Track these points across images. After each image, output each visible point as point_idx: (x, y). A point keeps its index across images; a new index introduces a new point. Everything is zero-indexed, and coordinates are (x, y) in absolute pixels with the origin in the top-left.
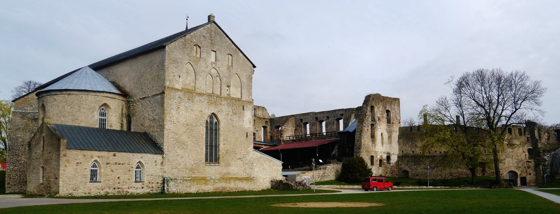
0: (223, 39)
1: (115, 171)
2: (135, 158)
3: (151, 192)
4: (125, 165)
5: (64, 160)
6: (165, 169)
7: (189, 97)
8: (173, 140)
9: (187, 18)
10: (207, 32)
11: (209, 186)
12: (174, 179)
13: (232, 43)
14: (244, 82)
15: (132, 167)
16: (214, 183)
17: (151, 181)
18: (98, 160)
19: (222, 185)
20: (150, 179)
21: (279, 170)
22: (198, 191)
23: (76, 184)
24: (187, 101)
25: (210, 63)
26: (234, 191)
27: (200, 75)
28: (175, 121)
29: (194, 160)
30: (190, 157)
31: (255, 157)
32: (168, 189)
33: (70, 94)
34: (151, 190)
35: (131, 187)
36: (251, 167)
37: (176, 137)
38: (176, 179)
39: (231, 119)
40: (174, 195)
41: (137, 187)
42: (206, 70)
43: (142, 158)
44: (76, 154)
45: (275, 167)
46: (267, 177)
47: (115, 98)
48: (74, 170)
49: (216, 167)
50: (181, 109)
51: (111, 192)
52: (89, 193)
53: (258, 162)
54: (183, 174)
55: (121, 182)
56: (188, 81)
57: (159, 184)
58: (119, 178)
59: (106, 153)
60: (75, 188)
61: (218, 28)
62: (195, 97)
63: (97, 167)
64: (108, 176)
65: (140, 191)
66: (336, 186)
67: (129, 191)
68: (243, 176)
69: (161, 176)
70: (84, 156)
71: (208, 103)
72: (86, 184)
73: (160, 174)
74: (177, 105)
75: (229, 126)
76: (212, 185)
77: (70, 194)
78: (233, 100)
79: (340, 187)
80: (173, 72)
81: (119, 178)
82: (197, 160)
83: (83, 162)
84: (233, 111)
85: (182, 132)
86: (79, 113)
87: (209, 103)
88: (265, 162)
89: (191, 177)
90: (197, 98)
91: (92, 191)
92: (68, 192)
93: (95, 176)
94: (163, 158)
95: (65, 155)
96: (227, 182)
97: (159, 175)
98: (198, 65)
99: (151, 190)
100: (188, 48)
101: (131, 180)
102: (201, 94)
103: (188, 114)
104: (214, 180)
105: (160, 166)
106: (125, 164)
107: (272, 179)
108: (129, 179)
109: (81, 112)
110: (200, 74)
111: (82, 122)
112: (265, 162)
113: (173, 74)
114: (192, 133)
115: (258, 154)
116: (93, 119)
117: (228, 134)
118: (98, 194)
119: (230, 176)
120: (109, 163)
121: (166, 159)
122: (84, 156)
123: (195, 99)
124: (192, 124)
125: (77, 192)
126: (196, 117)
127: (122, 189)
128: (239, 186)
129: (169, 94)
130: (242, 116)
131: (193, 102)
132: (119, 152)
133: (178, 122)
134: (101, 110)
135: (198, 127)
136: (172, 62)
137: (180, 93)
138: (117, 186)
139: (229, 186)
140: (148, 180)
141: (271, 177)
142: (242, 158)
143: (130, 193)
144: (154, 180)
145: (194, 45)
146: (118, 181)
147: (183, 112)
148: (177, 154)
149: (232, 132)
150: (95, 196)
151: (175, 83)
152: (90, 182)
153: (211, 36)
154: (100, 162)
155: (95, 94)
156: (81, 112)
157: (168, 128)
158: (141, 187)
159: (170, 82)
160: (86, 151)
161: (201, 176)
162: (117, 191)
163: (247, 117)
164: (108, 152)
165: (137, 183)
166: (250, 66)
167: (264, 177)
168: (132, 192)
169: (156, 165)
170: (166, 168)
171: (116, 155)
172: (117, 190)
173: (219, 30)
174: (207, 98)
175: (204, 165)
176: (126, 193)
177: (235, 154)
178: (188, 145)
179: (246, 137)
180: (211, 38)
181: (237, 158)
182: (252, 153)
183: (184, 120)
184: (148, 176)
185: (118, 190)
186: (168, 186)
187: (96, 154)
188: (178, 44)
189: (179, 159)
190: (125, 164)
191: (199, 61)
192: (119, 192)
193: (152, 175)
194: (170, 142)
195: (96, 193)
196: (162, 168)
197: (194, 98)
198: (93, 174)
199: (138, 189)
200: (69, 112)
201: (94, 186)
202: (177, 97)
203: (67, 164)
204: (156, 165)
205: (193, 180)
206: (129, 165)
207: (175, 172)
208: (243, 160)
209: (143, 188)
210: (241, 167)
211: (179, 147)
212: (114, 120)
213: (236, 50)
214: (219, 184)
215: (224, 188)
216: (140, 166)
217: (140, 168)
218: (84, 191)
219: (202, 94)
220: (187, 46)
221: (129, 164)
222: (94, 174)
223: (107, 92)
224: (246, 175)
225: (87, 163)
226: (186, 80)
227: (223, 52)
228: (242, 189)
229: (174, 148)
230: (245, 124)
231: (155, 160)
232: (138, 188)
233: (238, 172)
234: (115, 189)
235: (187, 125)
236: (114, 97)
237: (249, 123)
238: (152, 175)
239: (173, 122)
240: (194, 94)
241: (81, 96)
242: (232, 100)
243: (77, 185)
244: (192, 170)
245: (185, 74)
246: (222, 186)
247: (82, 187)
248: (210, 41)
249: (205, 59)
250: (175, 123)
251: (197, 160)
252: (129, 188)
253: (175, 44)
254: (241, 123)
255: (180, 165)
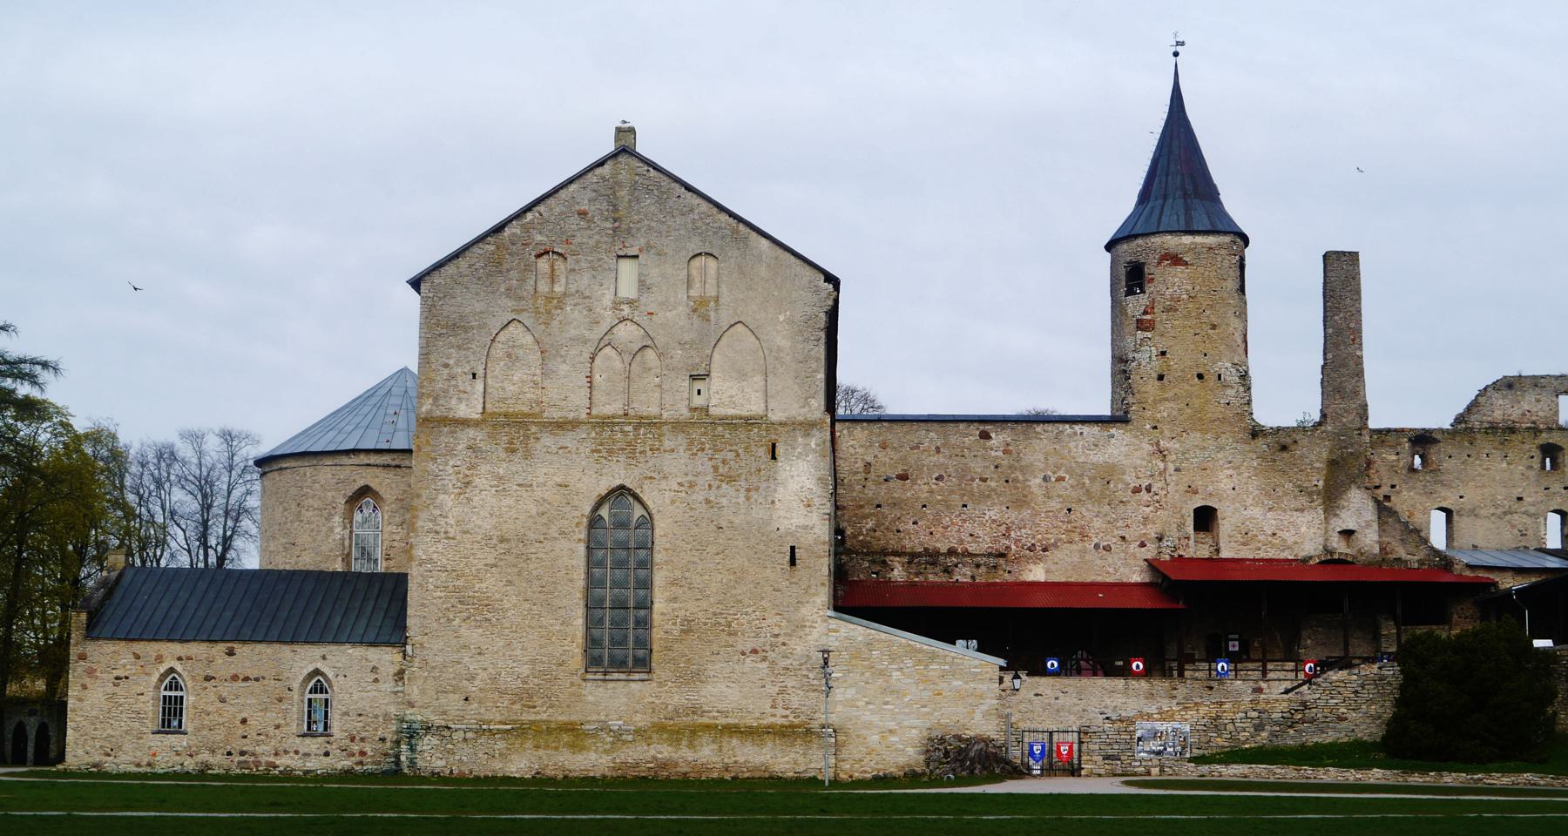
0: (671, 203)
1: (232, 702)
2: (302, 660)
3: (358, 768)
4: (265, 682)
5: (79, 669)
6: (408, 695)
7: (512, 443)
8: (442, 594)
9: (1173, 49)
10: (594, 194)
11: (593, 756)
12: (438, 727)
13: (715, 210)
14: (780, 349)
15: (289, 689)
16: (613, 743)
17: (358, 731)
18: (179, 668)
19: (653, 752)
20: (355, 725)
21: (981, 697)
22: (538, 773)
23: (112, 736)
24: (503, 455)
25: (610, 304)
26: (715, 775)
27: (561, 356)
28: (450, 530)
29: (533, 662)
30: (514, 653)
31: (837, 644)
32: (412, 762)
33: (281, 469)
34: (357, 764)
35: (286, 752)
36: (815, 682)
37: (457, 583)
38: (449, 728)
39: (708, 501)
40: (436, 777)
41: (306, 750)
42: (587, 333)
43: (324, 658)
44: (114, 652)
45: (955, 683)
46: (905, 723)
47: (399, 467)
48: (107, 697)
49: (633, 685)
50: (476, 487)
51: (218, 762)
52: (149, 765)
53: (854, 662)
54: (483, 711)
55: (252, 734)
56: (511, 388)
57: (388, 744)
58: (244, 721)
59: (204, 646)
60: (109, 750)
61: (646, 168)
62: (538, 439)
63: (182, 690)
64: (209, 714)
65: (317, 764)
66: (1278, 771)
67: (278, 763)
68: (773, 720)
69: (393, 717)
70: (137, 657)
71: (593, 451)
72: (141, 738)
73: (393, 710)
74: (461, 476)
75: (696, 530)
76: (607, 752)
77: (95, 766)
78: (720, 428)
79: (1294, 774)
80: (446, 366)
81: (244, 721)
82: (544, 663)
83: (134, 674)
84: (716, 468)
85: (480, 566)
86: (298, 523)
87: (599, 451)
88: (893, 660)
89: (514, 722)
90: (547, 440)
91: (157, 759)
92: (90, 760)
93: (175, 715)
94: (404, 658)
95: (83, 657)
96: (678, 741)
97: (386, 715)
98: (555, 323)
99: (357, 764)
100: (508, 270)
101: (284, 729)
102: (561, 426)
103: (511, 502)
104: (618, 736)
105: (393, 684)
106: (264, 678)
107: (937, 733)
108: (277, 727)
109: (301, 521)
110: (563, 353)
111: (305, 550)
112: (893, 660)
113: (446, 371)
114: (524, 565)
115: (857, 631)
116: (330, 541)
117: (696, 559)
118: (178, 768)
119: (705, 720)
120: (214, 678)
121: (417, 660)
122: (137, 657)
123: (538, 446)
124: (525, 535)
125: (115, 761)
126: (541, 509)
127: (253, 754)
128: (741, 759)
129: (427, 441)
130: (763, 485)
131: (528, 455)
132: (244, 642)
133: (465, 532)
134: (361, 507)
135: (548, 545)
136: (444, 331)
137: (471, 432)
138: (238, 745)
139: (689, 755)
140: (346, 731)
141: (928, 725)
142: (768, 648)
143: (281, 769)
144: (366, 731)
145: (539, 256)
146: (240, 732)
147: (484, 494)
148: (462, 641)
149: (712, 549)
150: (167, 773)
151: (454, 401)
152: (153, 733)
153: (614, 206)
154: (185, 674)
155: (336, 461)
156: (301, 521)
157: (424, 557)
158: (322, 753)
159: (436, 399)
160: (142, 643)
161: (560, 718)
162: (239, 762)
163: (793, 486)
164: (207, 644)
165: (308, 740)
166: (810, 282)
167: (892, 725)
168: (288, 766)
169: (376, 680)
170: (414, 691)
171: (237, 651)
172: (237, 758)
173: (653, 173)
174: (594, 435)
175: (576, 679)
176: (265, 769)
177: (730, 634)
178: (505, 611)
179: (787, 566)
180: (616, 210)
181: (740, 647)
182: (820, 627)
183: (487, 525)
184: (346, 717)
185: (242, 758)
186: (412, 749)
187: (171, 653)
188: (470, 266)
189: (466, 659)
190: (264, 678)
191: (556, 308)
192: (244, 765)
193: (360, 715)
194: (433, 604)
195: (170, 765)
196: (397, 692)
197: (532, 440)
198: (170, 709)
199: (311, 758)
200: (280, 524)
201: (164, 744)
202: (460, 447)
203: (87, 681)
204: (376, 680)
205: (519, 731)
206: (279, 683)
207: (453, 702)
208: (771, 655)
209: (327, 754)
210: (760, 683)
211: (469, 618)
212: (398, 538)
213: (735, 231)
214: (639, 749)
215: (664, 765)
216: (318, 684)
217: (327, 692)
218: (135, 757)
219: (570, 422)
220: (506, 266)
221: (281, 678)
222: (171, 712)
223: (367, 451)
224: (786, 717)
225: (146, 678)
226: (506, 384)
227: (669, 251)
228: (757, 769)
229: (450, 621)
230: (782, 513)
231: (374, 663)
232: (309, 755)
233: (744, 702)
234: (229, 754)
235: (502, 540)
236: (394, 463)
237: (804, 511)
238: (360, 715)
239: (443, 536)
240: (534, 429)
241: (302, 470)
242: (715, 429)
243: (114, 740)
244: (525, 697)
245: (502, 363)
246: (654, 757)
247: (127, 747)
248: (609, 225)
249: (588, 294)
250: (453, 539)
251: (544, 663)
252: (276, 754)
253: (458, 268)
254: (758, 513)
255: (472, 678)
